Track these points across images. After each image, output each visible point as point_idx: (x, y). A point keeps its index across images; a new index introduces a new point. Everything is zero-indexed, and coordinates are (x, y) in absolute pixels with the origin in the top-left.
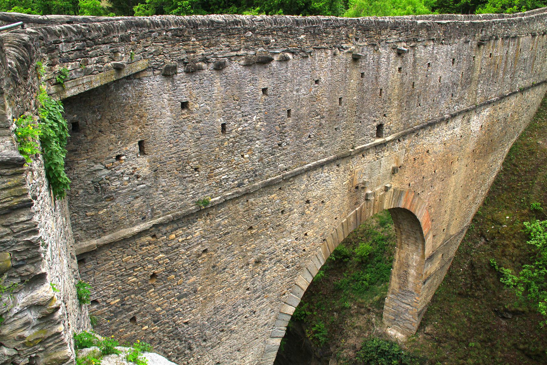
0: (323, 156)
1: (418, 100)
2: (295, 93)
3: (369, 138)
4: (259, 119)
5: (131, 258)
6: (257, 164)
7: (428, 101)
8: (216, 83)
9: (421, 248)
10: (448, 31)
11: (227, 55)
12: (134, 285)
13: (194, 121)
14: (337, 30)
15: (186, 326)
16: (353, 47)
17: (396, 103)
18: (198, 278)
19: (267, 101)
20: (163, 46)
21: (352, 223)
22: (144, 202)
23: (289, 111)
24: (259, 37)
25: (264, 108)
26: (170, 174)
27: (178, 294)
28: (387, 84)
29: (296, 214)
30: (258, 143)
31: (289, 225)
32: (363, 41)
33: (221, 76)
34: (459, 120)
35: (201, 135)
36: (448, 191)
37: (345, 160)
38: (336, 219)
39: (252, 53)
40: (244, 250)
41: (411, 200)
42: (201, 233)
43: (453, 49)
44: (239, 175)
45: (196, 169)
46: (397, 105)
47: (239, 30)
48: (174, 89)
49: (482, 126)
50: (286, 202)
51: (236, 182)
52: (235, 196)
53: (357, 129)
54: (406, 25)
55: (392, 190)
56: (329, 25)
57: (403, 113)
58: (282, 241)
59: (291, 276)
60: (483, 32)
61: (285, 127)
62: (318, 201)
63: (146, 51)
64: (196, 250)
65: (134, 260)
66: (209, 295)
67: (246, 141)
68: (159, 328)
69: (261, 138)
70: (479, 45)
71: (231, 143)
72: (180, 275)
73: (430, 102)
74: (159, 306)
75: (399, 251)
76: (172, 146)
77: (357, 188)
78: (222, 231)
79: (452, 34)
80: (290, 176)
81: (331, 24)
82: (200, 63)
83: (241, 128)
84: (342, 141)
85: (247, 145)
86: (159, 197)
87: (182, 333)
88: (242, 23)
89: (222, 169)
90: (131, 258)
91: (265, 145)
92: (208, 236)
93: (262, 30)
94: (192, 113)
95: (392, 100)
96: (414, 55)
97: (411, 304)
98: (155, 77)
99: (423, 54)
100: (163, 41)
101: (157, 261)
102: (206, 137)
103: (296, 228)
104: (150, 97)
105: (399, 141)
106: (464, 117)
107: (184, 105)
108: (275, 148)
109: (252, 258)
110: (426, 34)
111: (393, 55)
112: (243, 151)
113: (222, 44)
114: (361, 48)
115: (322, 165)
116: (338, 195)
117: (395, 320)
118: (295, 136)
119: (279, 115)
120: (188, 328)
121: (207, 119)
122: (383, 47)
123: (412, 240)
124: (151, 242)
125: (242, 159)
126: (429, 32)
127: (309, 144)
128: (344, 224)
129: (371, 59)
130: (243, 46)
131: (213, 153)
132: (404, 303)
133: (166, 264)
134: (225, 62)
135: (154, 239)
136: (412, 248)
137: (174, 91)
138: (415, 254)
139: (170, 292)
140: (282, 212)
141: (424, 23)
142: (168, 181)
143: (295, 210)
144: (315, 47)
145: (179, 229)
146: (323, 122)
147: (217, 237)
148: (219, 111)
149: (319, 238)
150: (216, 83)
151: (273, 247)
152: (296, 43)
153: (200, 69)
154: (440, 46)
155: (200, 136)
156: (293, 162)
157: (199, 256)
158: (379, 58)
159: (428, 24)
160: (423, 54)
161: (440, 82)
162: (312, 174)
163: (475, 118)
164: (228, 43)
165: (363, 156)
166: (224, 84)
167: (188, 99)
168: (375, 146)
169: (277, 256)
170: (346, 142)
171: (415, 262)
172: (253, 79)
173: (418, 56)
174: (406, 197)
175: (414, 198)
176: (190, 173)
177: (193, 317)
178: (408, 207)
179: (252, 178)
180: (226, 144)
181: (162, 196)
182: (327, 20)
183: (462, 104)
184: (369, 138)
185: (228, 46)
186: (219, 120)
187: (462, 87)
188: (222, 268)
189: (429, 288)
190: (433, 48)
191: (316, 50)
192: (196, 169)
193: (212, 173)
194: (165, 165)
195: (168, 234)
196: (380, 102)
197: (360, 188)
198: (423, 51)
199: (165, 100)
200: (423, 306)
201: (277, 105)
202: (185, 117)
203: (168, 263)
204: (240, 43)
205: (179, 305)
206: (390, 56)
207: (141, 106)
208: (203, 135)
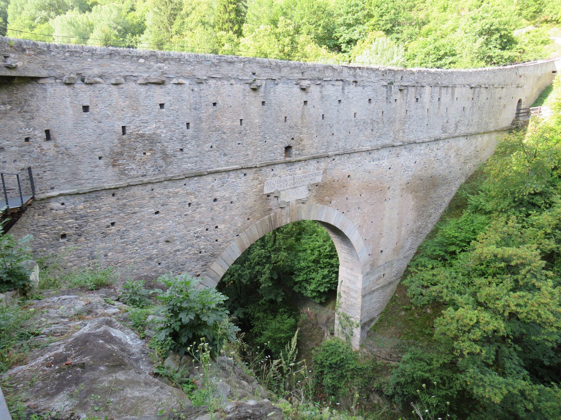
4: (159, 127)
61: (185, 136)
74: (71, 262)
95: (299, 127)
96: (321, 92)
101: (67, 224)
111: (296, 89)
119: (178, 126)
127: (212, 153)
135: (63, 206)
140: (190, 204)
146: (225, 136)
149: (232, 232)
157: (108, 227)
163: (406, 153)
173: (325, 93)
180: (127, 142)
199: (68, 103)
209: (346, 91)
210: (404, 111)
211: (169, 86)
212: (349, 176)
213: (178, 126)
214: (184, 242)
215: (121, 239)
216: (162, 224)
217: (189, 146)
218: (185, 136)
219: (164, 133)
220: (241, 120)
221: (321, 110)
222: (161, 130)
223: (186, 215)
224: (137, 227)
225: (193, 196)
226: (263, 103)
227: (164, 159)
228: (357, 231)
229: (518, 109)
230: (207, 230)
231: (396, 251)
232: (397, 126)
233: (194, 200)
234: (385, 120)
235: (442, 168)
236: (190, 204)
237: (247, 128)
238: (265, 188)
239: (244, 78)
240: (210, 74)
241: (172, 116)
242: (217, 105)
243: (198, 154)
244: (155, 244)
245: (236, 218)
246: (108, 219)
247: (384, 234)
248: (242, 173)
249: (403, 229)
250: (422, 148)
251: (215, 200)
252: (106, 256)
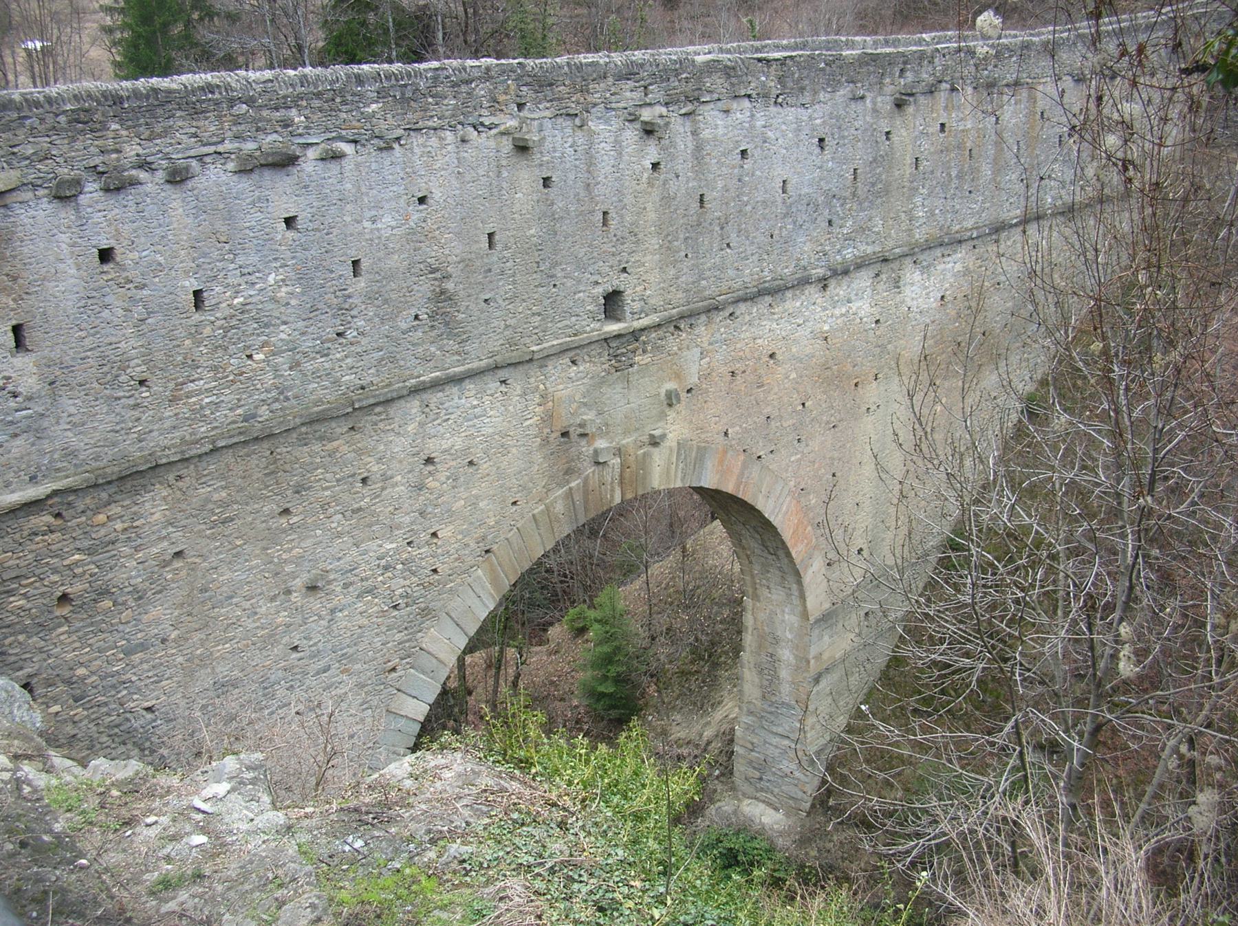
0: (458, 361)
1: (722, 235)
2: (367, 224)
3: (584, 323)
4: (283, 280)
5: (11, 558)
6: (286, 374)
7: (755, 237)
8: (174, 210)
9: (796, 594)
10: (793, 74)
11: (192, 153)
12: (22, 614)
13: (131, 286)
14: (464, 88)
15: (149, 716)
16: (512, 123)
17: (654, 242)
18: (169, 611)
19: (298, 243)
20: (50, 143)
21: (561, 516)
22: (33, 444)
23: (356, 263)
24: (265, 113)
25: (293, 258)
26: (84, 390)
27: (124, 642)
28: (620, 201)
29: (403, 488)
30: (284, 333)
31: (384, 510)
32: (538, 108)
33: (184, 195)
34: (863, 280)
35: (149, 313)
36: (857, 453)
37: (520, 368)
38: (514, 503)
39: (250, 146)
40: (276, 560)
41: (736, 471)
42: (165, 516)
43: (816, 115)
44: (244, 396)
45: (142, 383)
46: (656, 247)
47: (217, 103)
48: (79, 223)
49: (943, 297)
50: (369, 459)
51: (240, 411)
52: (235, 440)
53: (546, 302)
54: (661, 67)
55: (671, 441)
56: (441, 79)
57: (678, 265)
58: (373, 545)
59: (406, 629)
60: (908, 74)
61: (350, 297)
62: (459, 460)
63: (14, 154)
64: (157, 551)
65: (18, 561)
66: (198, 652)
67: (256, 325)
68: (85, 713)
69: (291, 319)
70: (899, 105)
71: (220, 329)
72: (124, 603)
73: (761, 239)
75: (754, 605)
76: (83, 334)
77: (565, 434)
78: (216, 514)
79: (807, 82)
81: (447, 77)
82: (134, 172)
83: (241, 300)
84: (507, 326)
85: (258, 335)
86: (62, 435)
87: (141, 730)
88: (223, 90)
89: (202, 382)
90: (11, 558)
91: (303, 334)
92: (183, 523)
93: (271, 100)
94: (124, 270)
95: (641, 236)
96: (694, 133)
97: (790, 735)
98: (39, 202)
99: (721, 131)
100: (51, 133)
103: (407, 519)
104: (31, 240)
105: (677, 328)
106: (877, 275)
107: (105, 255)
108: (329, 340)
109: (298, 580)
110: (726, 85)
111: (631, 135)
112: (249, 347)
113: (181, 131)
114: (536, 123)
115: (457, 380)
116: (514, 450)
117: (761, 779)
118: (377, 315)
119: (332, 272)
120: (155, 721)
121: (160, 282)
122: (599, 118)
123: (774, 575)
124: (52, 528)
125: (249, 362)
126: (734, 80)
128: (537, 517)
129: (567, 145)
130: (229, 134)
131: (177, 349)
132: (776, 734)
133: (91, 576)
134: (187, 169)
135: (60, 522)
136: (777, 595)
137: (82, 228)
138: (787, 610)
139: (103, 636)
140: (364, 480)
141: (714, 61)
142: (81, 404)
143: (399, 478)
144: (408, 127)
145: (113, 505)
146: (450, 286)
147: (203, 527)
148: (185, 264)
149: (473, 545)
150: (174, 210)
151: (348, 558)
152: (359, 121)
153: (134, 183)
154: (773, 109)
155: (146, 316)
156: (378, 371)
157: (165, 564)
158: (591, 144)
159: (729, 63)
160: (721, 131)
161: (784, 192)
162: (434, 398)
163: (917, 276)
164: (193, 130)
165: (574, 362)
166: (194, 211)
168: (606, 339)
169: (362, 580)
170: (520, 330)
171: (790, 630)
172: (259, 198)
173: (706, 134)
174: (721, 462)
175: (745, 466)
176: (130, 390)
177: (165, 698)
178: (729, 488)
179: (277, 404)
180: (207, 331)
181: (69, 434)
182: (437, 69)
183: (867, 244)
184: (584, 323)
185: (195, 135)
186: (187, 283)
187: (860, 204)
188: (225, 595)
189: (834, 695)
190: (752, 116)
191: (412, 133)
192: (142, 383)
193: (181, 389)
194: (73, 371)
195: (89, 512)
196: (605, 240)
197: (573, 436)
198: (719, 122)
199: (64, 246)
200: (822, 741)
201: (323, 250)
202: (110, 277)
203: (96, 574)
204: (222, 129)
205: (128, 668)
206: (623, 138)
207: (14, 257)
208: (151, 312)
212: (772, 356)
213: (332, 272)
214: (351, 584)
226: (547, 182)
242: (431, 201)
246: (166, 544)
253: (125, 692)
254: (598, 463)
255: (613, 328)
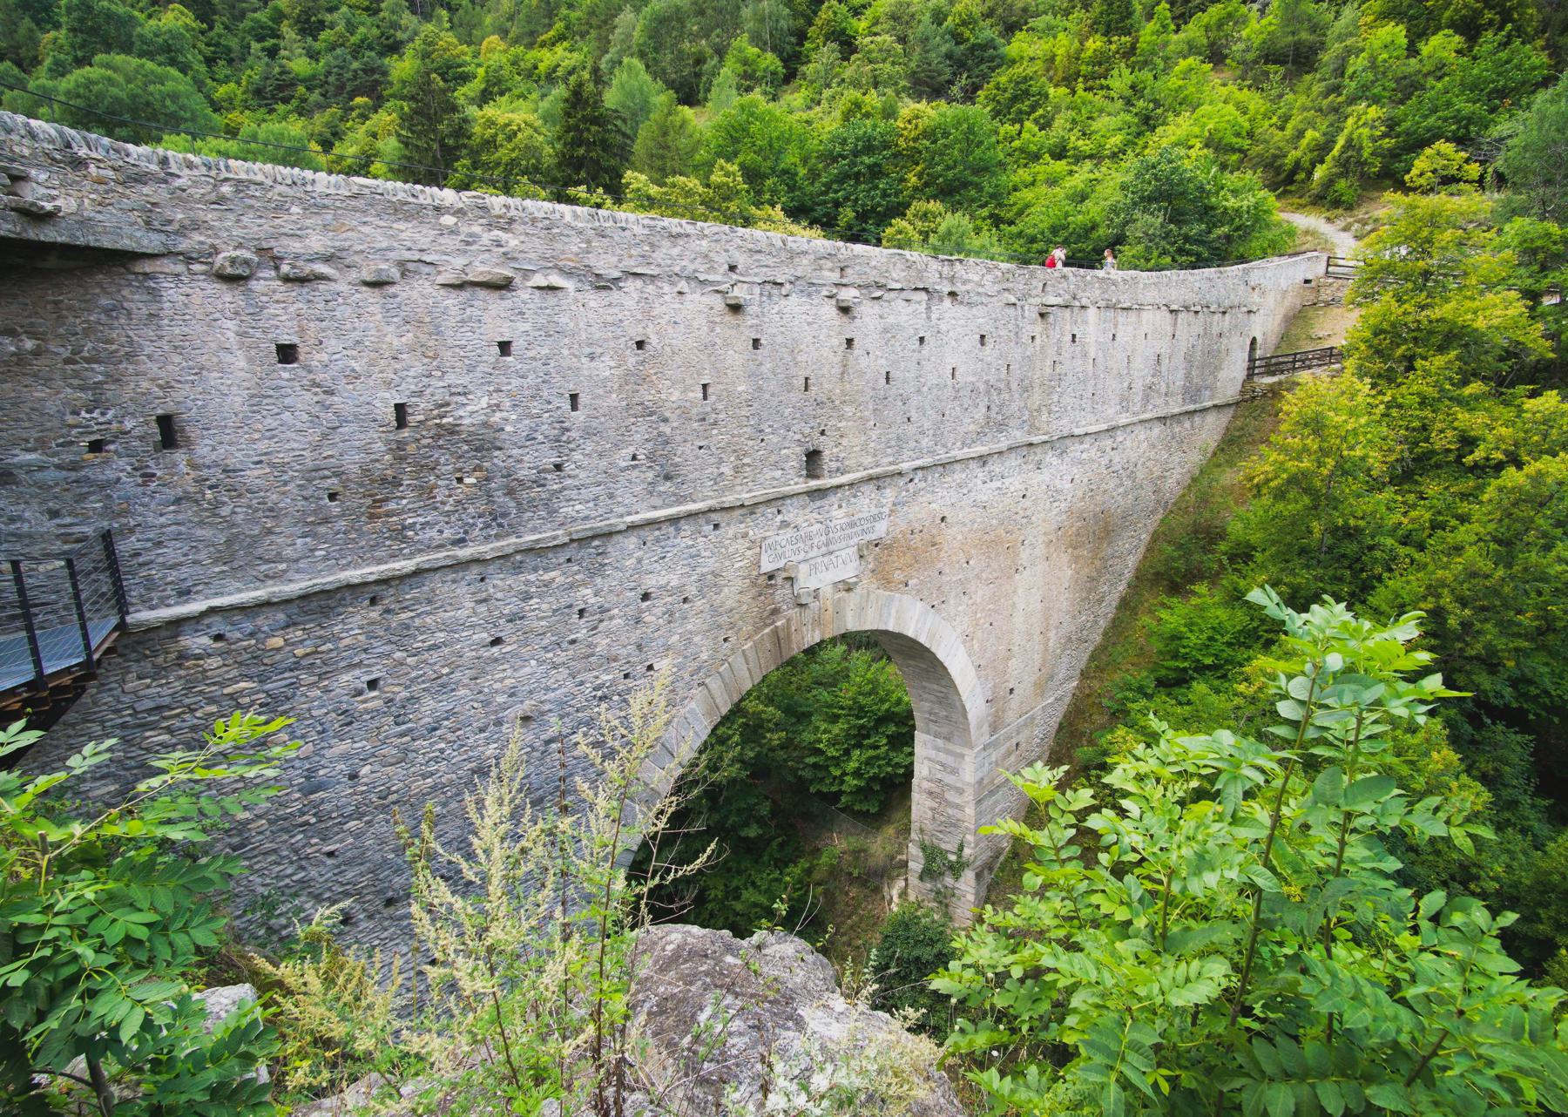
4: (498, 406)
5: (148, 687)
15: (329, 862)
23: (574, 398)
58: (589, 676)
61: (568, 430)
76: (257, 436)
80: (590, 534)
101: (231, 696)
102: (355, 426)
108: (545, 471)
111: (829, 311)
127: (635, 473)
140: (581, 612)
143: (616, 611)
146: (666, 429)
149: (687, 676)
150: (372, 315)
157: (360, 693)
163: (1055, 461)
167: (295, 340)
180: (411, 448)
186: (387, 395)
199: (230, 334)
209: (934, 316)
210: (1049, 362)
211: (524, 295)
212: (943, 519)
214: (568, 714)
215: (397, 724)
216: (509, 673)
217: (577, 456)
218: (568, 430)
219: (511, 422)
220: (705, 386)
221: (883, 361)
222: (505, 414)
223: (573, 642)
224: (442, 686)
225: (588, 591)
226: (756, 343)
227: (510, 492)
228: (962, 647)
229: (1252, 360)
230: (626, 676)
231: (1041, 688)
232: (1036, 398)
233: (592, 601)
234: (1014, 386)
235: (1121, 490)
236: (581, 612)
237: (720, 406)
238: (764, 559)
239: (711, 278)
240: (631, 264)
241: (532, 376)
242: (648, 347)
243: (601, 478)
244: (492, 728)
245: (696, 639)
246: (357, 672)
247: (1015, 649)
248: (708, 523)
249: (1052, 634)
250: (1085, 446)
251: (646, 597)
252: (353, 776)
253: (300, 836)
254: (801, 605)
255: (814, 484)
